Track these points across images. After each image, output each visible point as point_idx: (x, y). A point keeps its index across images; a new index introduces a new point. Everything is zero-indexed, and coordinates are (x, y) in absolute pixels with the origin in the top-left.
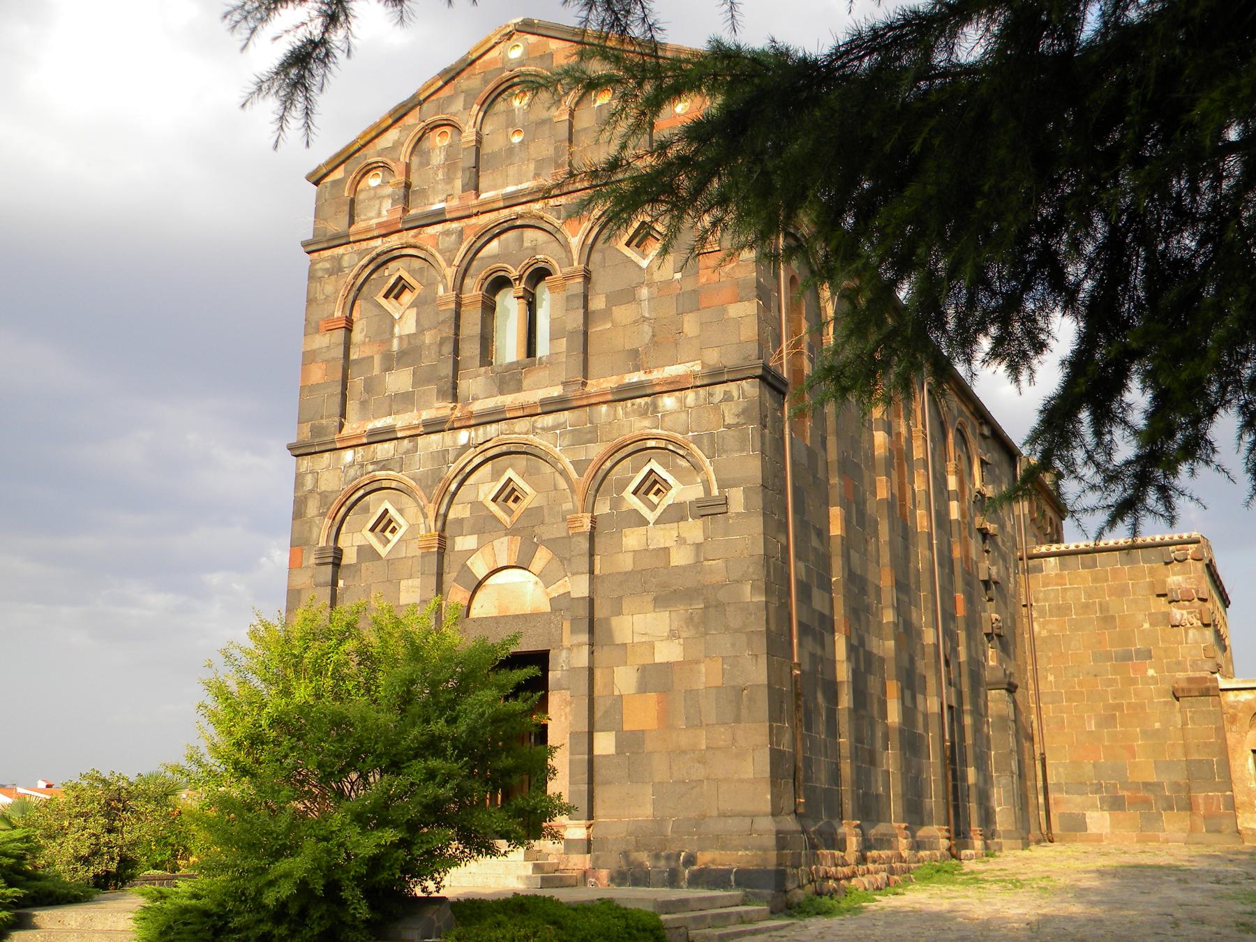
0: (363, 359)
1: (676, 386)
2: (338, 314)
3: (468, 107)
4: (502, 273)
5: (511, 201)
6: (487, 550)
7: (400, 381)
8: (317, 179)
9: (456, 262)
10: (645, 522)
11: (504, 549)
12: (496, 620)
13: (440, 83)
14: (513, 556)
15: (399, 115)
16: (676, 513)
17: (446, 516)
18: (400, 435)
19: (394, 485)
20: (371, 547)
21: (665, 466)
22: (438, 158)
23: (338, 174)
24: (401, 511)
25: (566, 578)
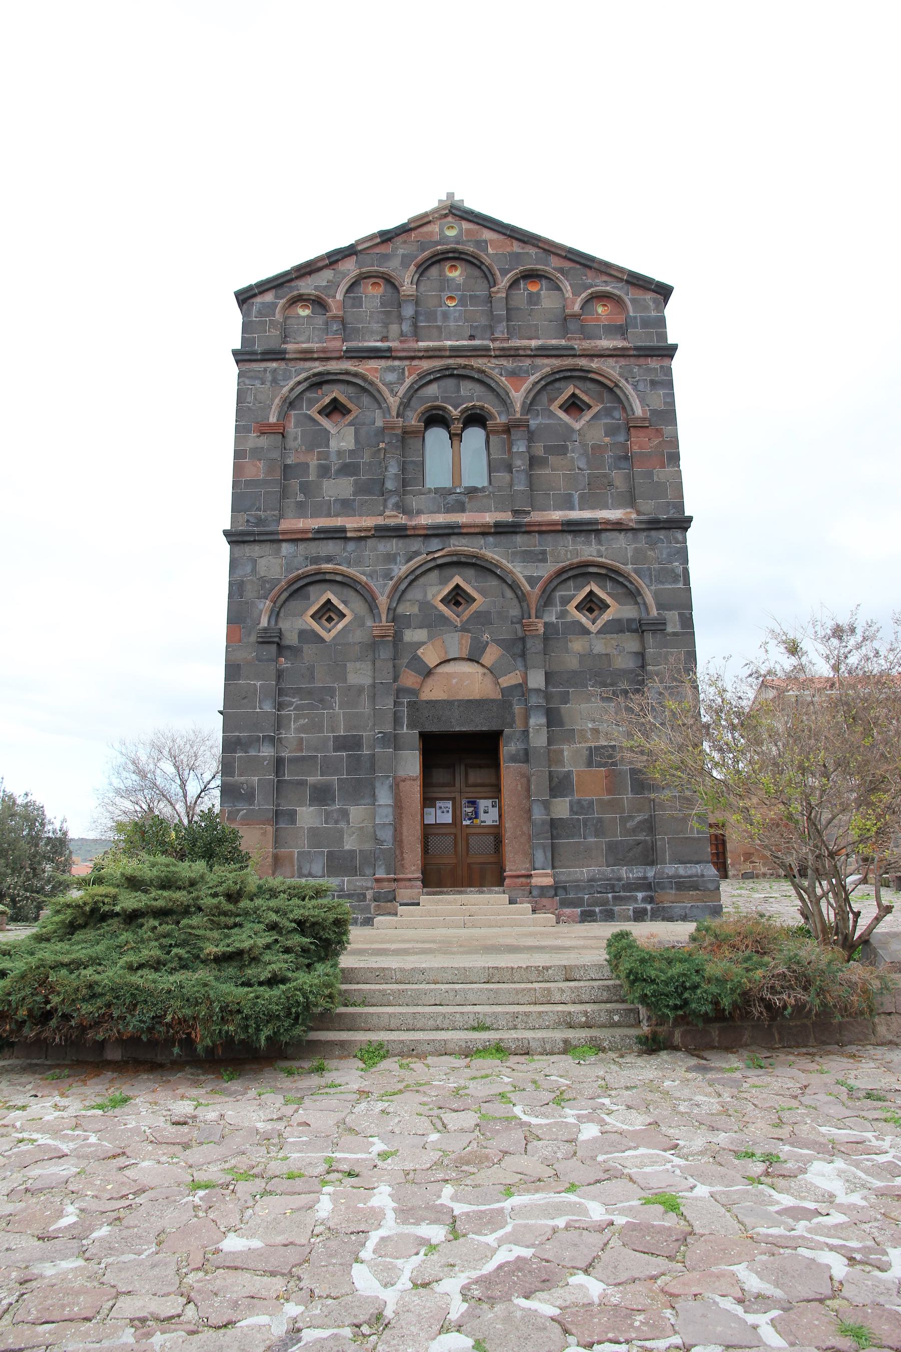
0: (298, 465)
1: (618, 527)
2: (273, 419)
3: (405, 265)
4: (441, 412)
5: (456, 352)
8: (244, 297)
9: (401, 393)
10: (586, 632)
11: (457, 644)
12: (449, 703)
13: (378, 240)
14: (464, 650)
17: (395, 609)
18: (349, 535)
19: (338, 578)
20: (313, 631)
21: (603, 588)
23: (269, 297)
24: (345, 603)
25: (517, 672)
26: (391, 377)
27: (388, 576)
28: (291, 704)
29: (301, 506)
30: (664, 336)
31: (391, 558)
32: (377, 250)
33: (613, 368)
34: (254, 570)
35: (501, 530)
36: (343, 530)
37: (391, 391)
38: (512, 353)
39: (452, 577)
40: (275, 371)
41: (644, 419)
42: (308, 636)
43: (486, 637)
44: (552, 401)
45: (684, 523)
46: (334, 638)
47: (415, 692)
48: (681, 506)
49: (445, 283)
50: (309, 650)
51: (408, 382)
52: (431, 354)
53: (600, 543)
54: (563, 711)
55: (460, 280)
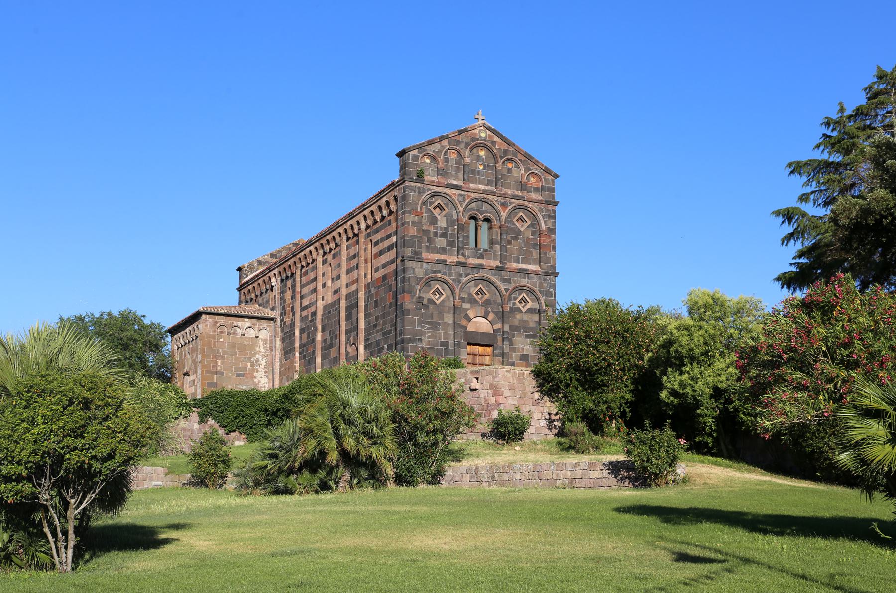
1: (535, 273)
5: (484, 192)
6: (474, 309)
7: (440, 242)
11: (481, 311)
15: (441, 139)
16: (530, 311)
19: (442, 280)
21: (527, 296)
22: (452, 163)
23: (415, 152)
24: (443, 290)
26: (461, 199)
27: (459, 281)
28: (425, 327)
29: (428, 247)
30: (553, 197)
31: (460, 275)
32: (455, 138)
33: (537, 207)
34: (414, 273)
35: (498, 269)
36: (445, 261)
37: (461, 205)
38: (504, 196)
39: (478, 285)
40: (419, 188)
41: (546, 231)
42: (431, 301)
43: (490, 309)
44: (514, 217)
45: (556, 274)
46: (440, 303)
47: (466, 328)
48: (554, 268)
49: (478, 158)
50: (431, 307)
51: (467, 201)
52: (476, 191)
53: (528, 279)
54: (513, 340)
55: (484, 157)
